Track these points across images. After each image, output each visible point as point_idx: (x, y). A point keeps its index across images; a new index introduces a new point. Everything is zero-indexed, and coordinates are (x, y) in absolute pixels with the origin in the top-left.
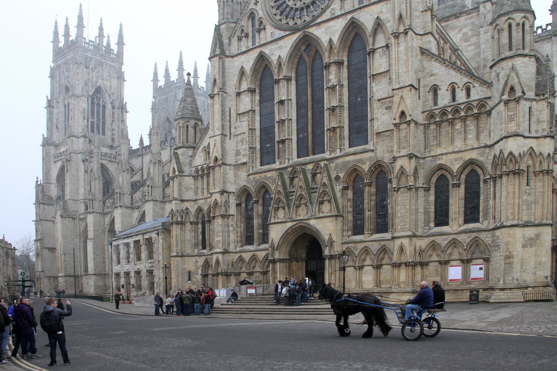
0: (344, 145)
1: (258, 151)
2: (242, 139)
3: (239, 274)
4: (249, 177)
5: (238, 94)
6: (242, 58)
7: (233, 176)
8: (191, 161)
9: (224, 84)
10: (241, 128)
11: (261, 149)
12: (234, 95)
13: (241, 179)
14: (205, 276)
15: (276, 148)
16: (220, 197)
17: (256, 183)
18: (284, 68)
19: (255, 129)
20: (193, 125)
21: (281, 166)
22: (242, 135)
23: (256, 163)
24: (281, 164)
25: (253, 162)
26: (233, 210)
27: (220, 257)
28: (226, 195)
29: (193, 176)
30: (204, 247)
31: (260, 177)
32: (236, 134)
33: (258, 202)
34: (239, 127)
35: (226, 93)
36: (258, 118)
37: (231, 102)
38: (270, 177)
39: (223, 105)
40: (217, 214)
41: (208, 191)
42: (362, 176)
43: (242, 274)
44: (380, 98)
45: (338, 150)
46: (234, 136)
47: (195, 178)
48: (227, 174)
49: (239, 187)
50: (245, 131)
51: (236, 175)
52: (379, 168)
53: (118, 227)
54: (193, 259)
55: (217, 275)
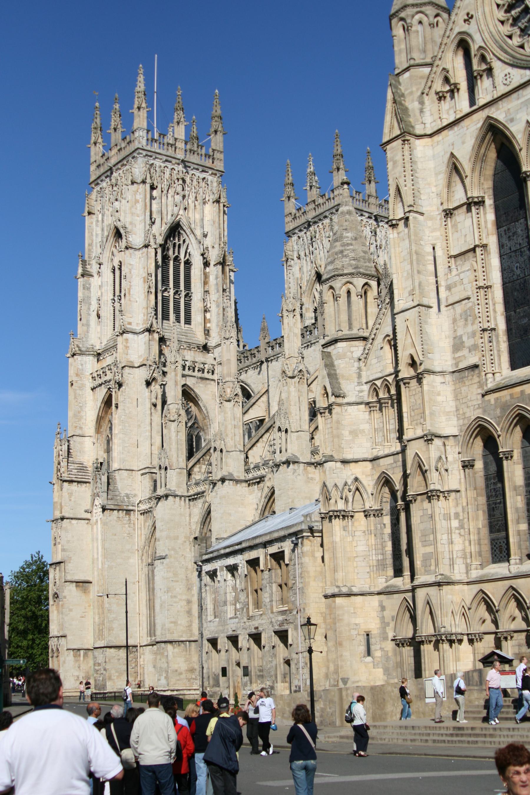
2: (465, 312)
4: (487, 398)
5: (448, 213)
7: (450, 397)
10: (459, 288)
11: (509, 330)
12: (439, 217)
13: (470, 404)
16: (424, 449)
19: (491, 287)
22: (464, 302)
23: (500, 364)
28: (437, 442)
29: (367, 404)
32: (451, 301)
33: (512, 457)
34: (456, 286)
35: (422, 214)
36: (495, 261)
46: (447, 306)
48: (439, 394)
49: (467, 422)
50: (469, 293)
51: (456, 398)
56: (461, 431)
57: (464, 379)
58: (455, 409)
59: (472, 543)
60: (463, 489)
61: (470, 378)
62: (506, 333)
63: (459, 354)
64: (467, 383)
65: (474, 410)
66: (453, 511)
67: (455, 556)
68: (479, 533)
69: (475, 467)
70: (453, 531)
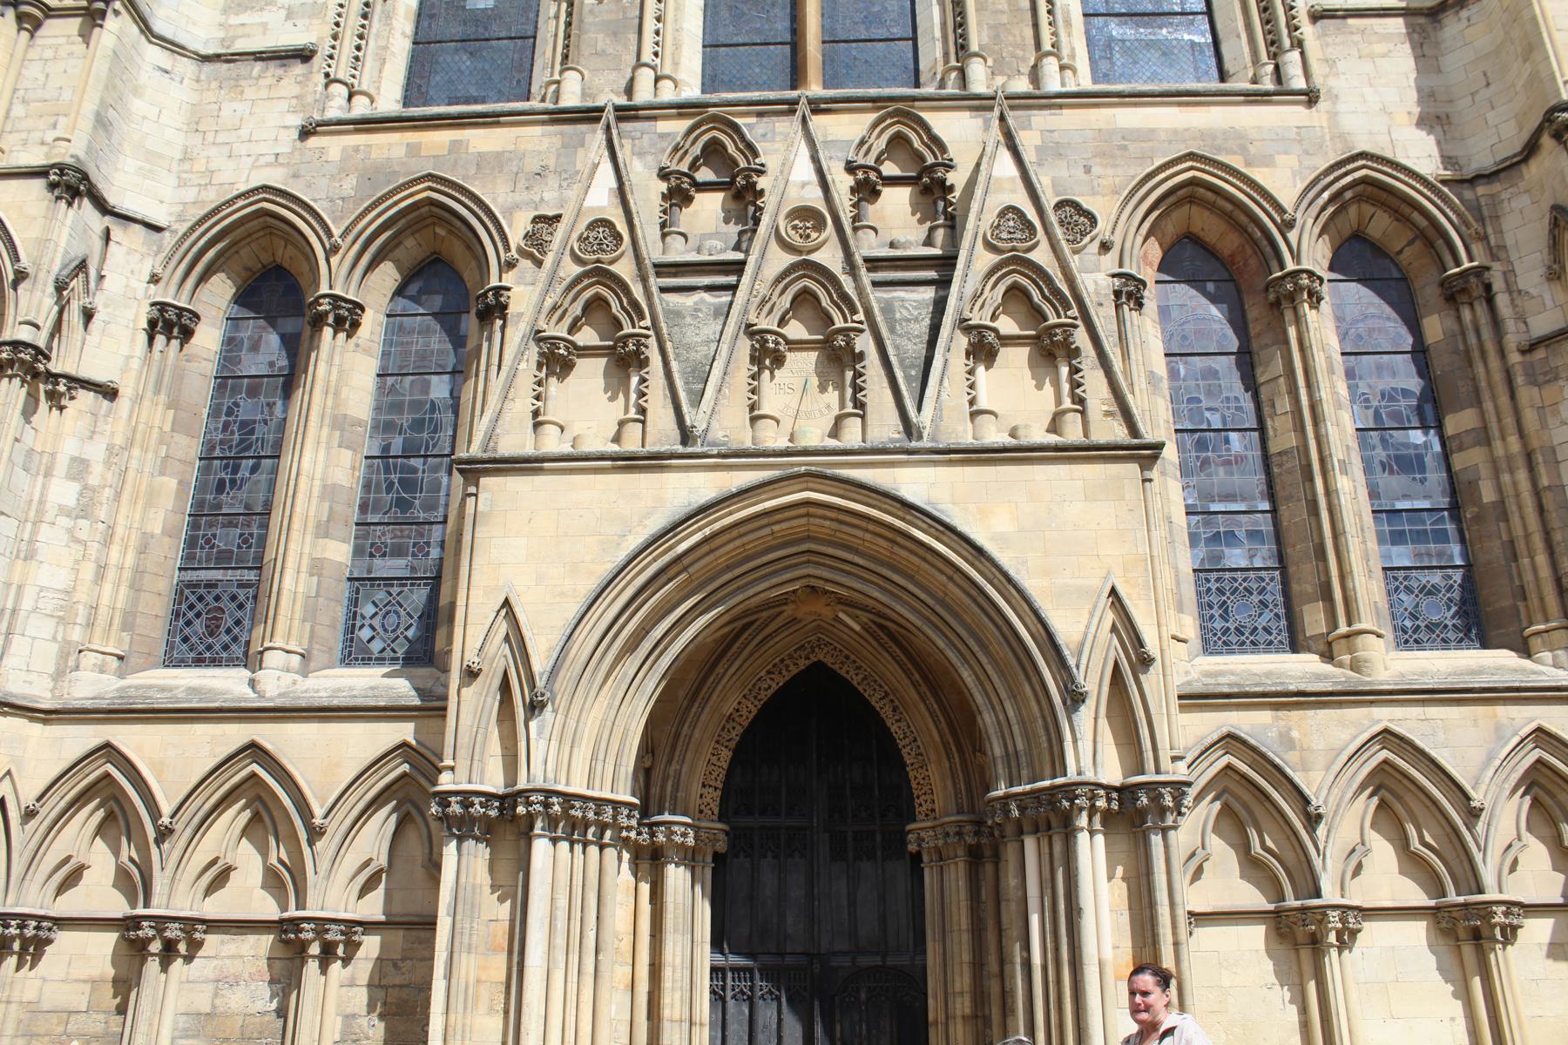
4: (313, 142)
13: (242, 149)
24: (584, 95)
33: (356, 325)
42: (1229, 243)
49: (213, 198)
52: (1353, 211)
56: (180, 218)
57: (243, 83)
58: (179, 156)
59: (111, 575)
60: (126, 392)
61: (262, 82)
62: (412, 17)
63: (245, 18)
64: (250, 93)
65: (254, 167)
66: (69, 448)
67: (27, 604)
68: (143, 550)
69: (195, 340)
70: (48, 517)
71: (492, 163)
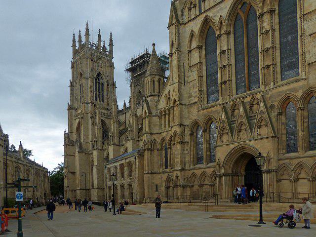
0: (277, 79)
1: (205, 93)
3: (193, 186)
6: (192, 24)
7: (187, 113)
8: (157, 105)
9: (179, 45)
14: (168, 188)
15: (220, 88)
17: (205, 116)
18: (224, 24)
20: (157, 80)
21: (224, 102)
25: (201, 101)
26: (187, 138)
27: (179, 173)
28: (182, 126)
30: (167, 167)
31: (208, 112)
37: (185, 59)
38: (215, 111)
39: (179, 61)
40: (176, 141)
41: (169, 126)
43: (195, 186)
44: (311, 33)
45: (272, 84)
47: (160, 117)
51: (189, 113)
53: (111, 157)
54: (159, 176)
55: (177, 187)
63: (191, 99)
71: (215, 112)
